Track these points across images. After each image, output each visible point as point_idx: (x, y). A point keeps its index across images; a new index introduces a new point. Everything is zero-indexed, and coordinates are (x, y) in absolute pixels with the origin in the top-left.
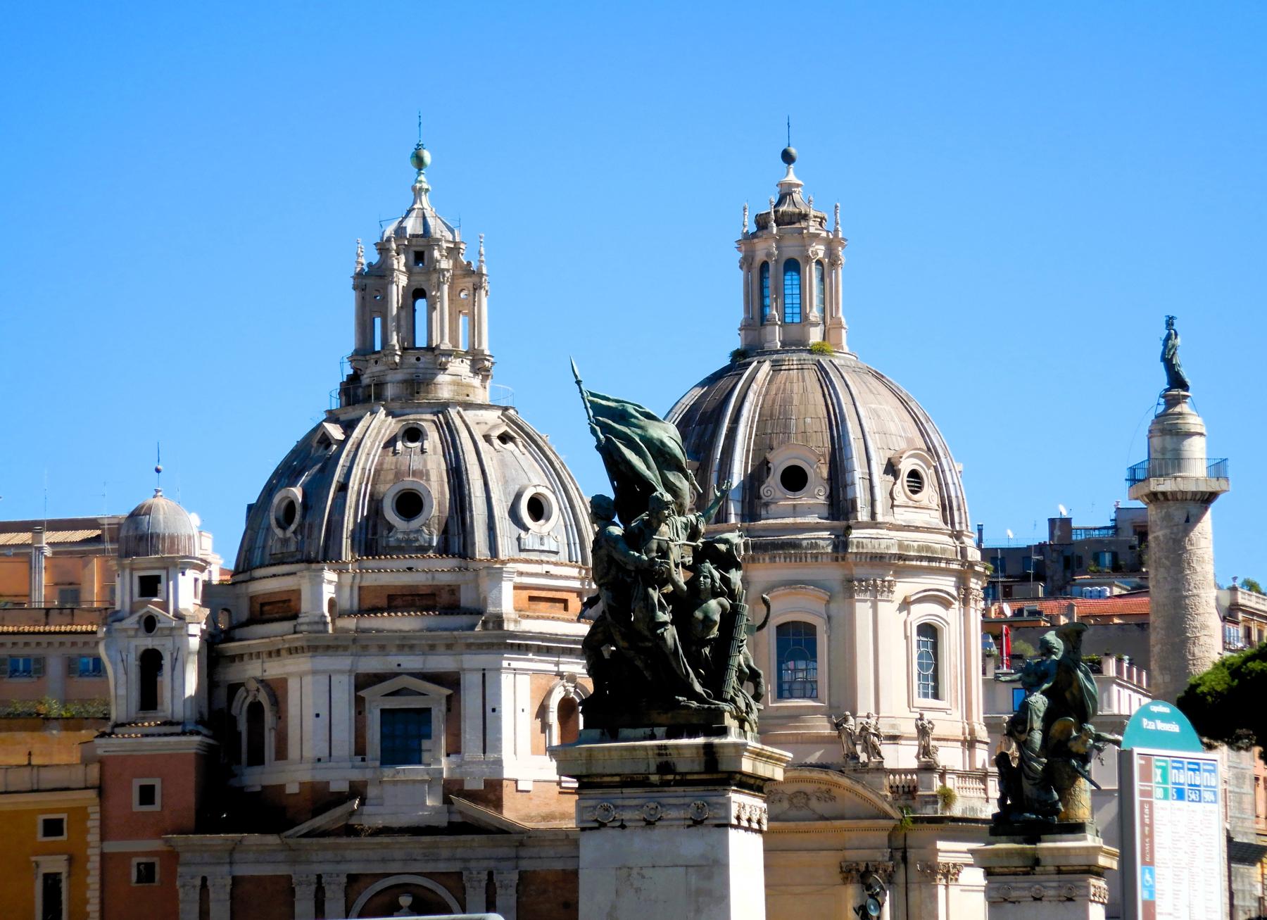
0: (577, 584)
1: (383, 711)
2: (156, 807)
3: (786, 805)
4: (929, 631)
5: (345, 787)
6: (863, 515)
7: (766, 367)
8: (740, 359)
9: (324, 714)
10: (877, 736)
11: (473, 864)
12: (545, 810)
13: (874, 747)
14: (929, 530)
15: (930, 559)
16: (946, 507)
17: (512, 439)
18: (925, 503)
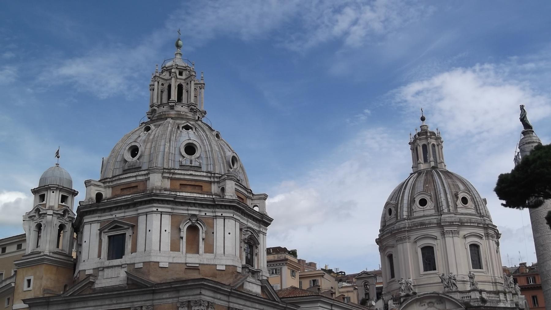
0: (207, 179)
1: (109, 237)
2: (31, 288)
3: (426, 306)
4: (475, 248)
5: (91, 272)
6: (446, 211)
7: (416, 174)
8: (411, 174)
9: (87, 241)
10: (455, 280)
11: (135, 303)
12: (175, 277)
13: (454, 284)
14: (470, 214)
15: (471, 223)
16: (476, 208)
17: (192, 128)
18: (470, 207)
